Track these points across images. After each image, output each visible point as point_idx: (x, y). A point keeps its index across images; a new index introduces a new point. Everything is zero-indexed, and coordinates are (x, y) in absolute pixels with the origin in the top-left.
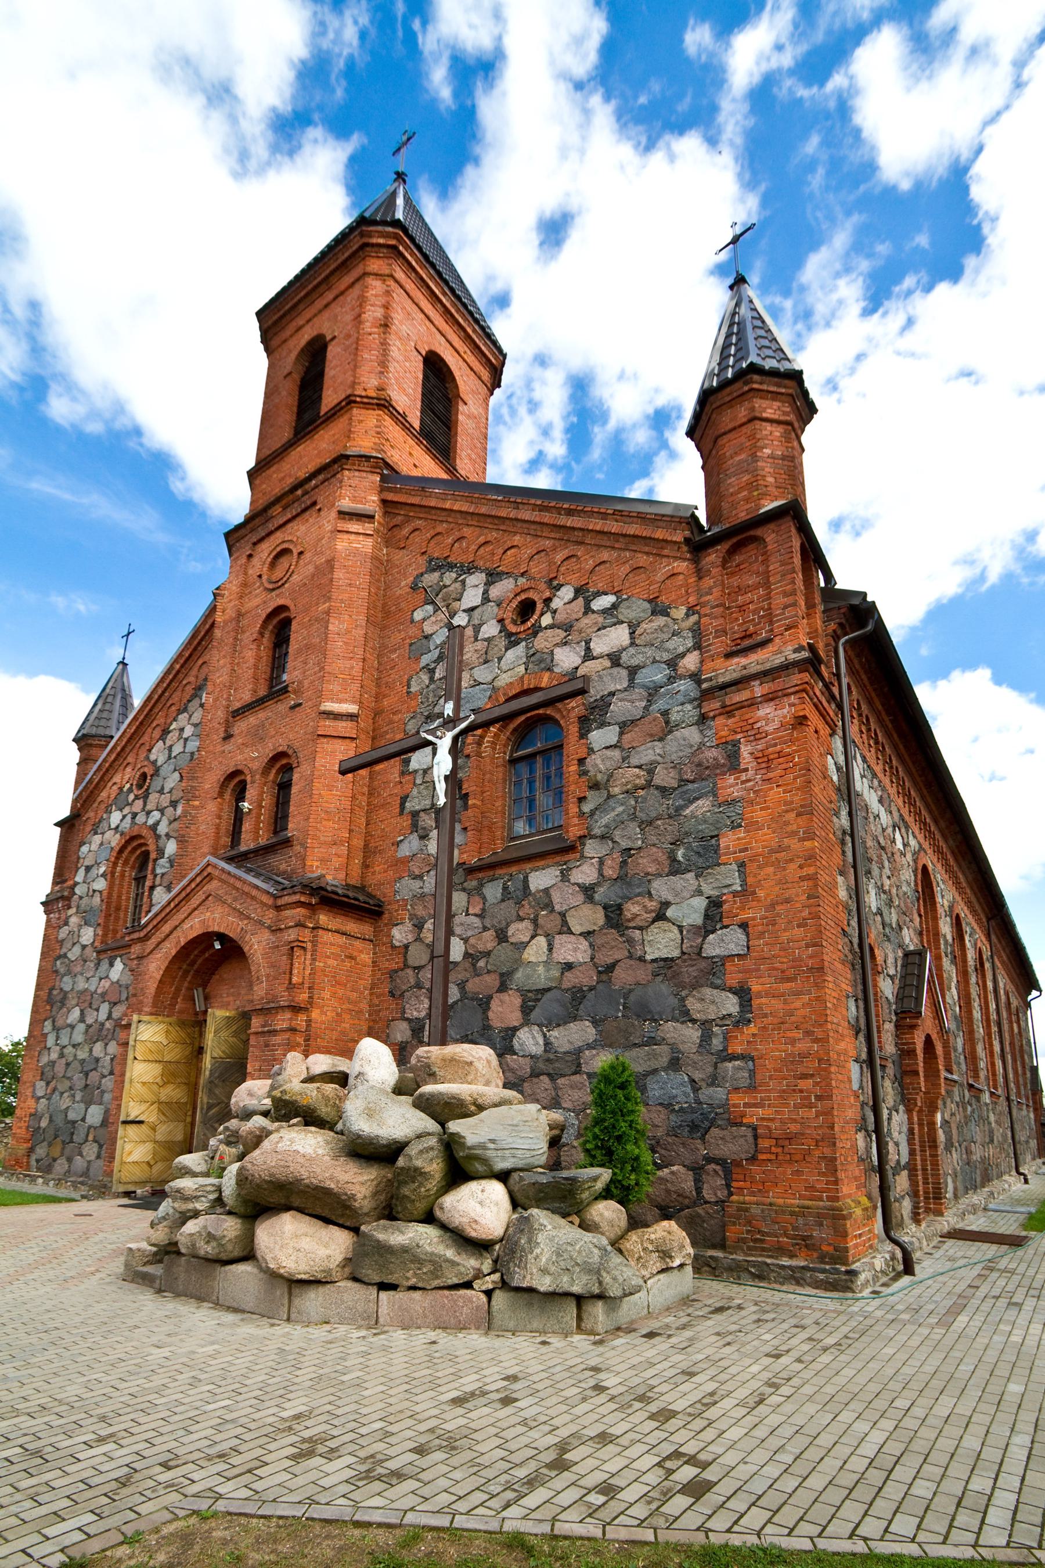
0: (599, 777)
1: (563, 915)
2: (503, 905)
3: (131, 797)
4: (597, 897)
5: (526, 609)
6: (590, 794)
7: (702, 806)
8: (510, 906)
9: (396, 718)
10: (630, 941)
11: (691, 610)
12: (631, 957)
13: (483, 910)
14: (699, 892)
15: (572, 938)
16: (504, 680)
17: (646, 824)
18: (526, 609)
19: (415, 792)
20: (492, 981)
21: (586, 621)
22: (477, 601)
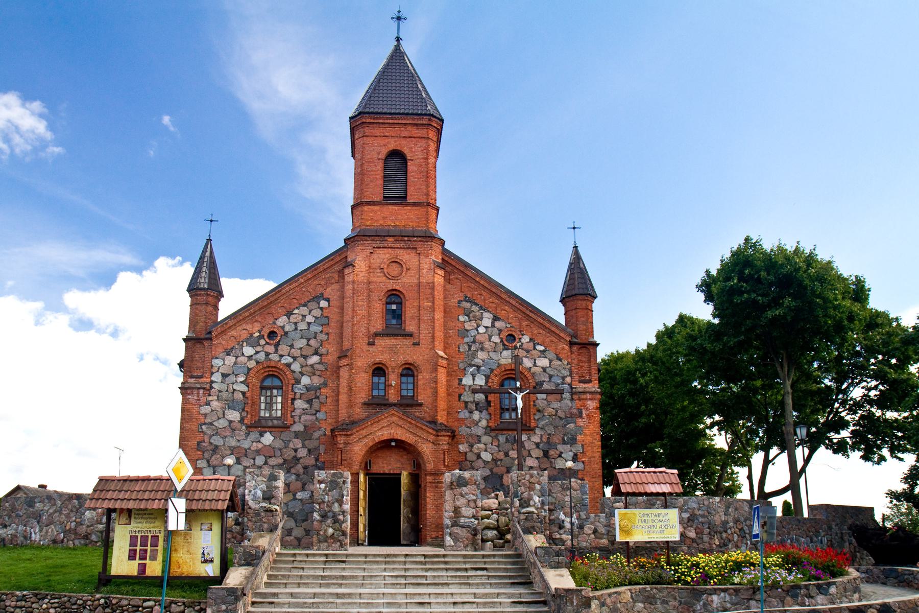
0: (540, 408)
1: (529, 451)
2: (507, 444)
3: (262, 342)
4: (540, 447)
5: (511, 337)
6: (538, 413)
7: (572, 426)
8: (508, 446)
9: (454, 360)
10: (551, 462)
11: (568, 364)
12: (551, 467)
13: (499, 444)
14: (571, 451)
15: (532, 459)
16: (503, 362)
17: (556, 427)
18: (511, 337)
19: (465, 393)
20: (504, 469)
21: (534, 352)
22: (490, 325)
